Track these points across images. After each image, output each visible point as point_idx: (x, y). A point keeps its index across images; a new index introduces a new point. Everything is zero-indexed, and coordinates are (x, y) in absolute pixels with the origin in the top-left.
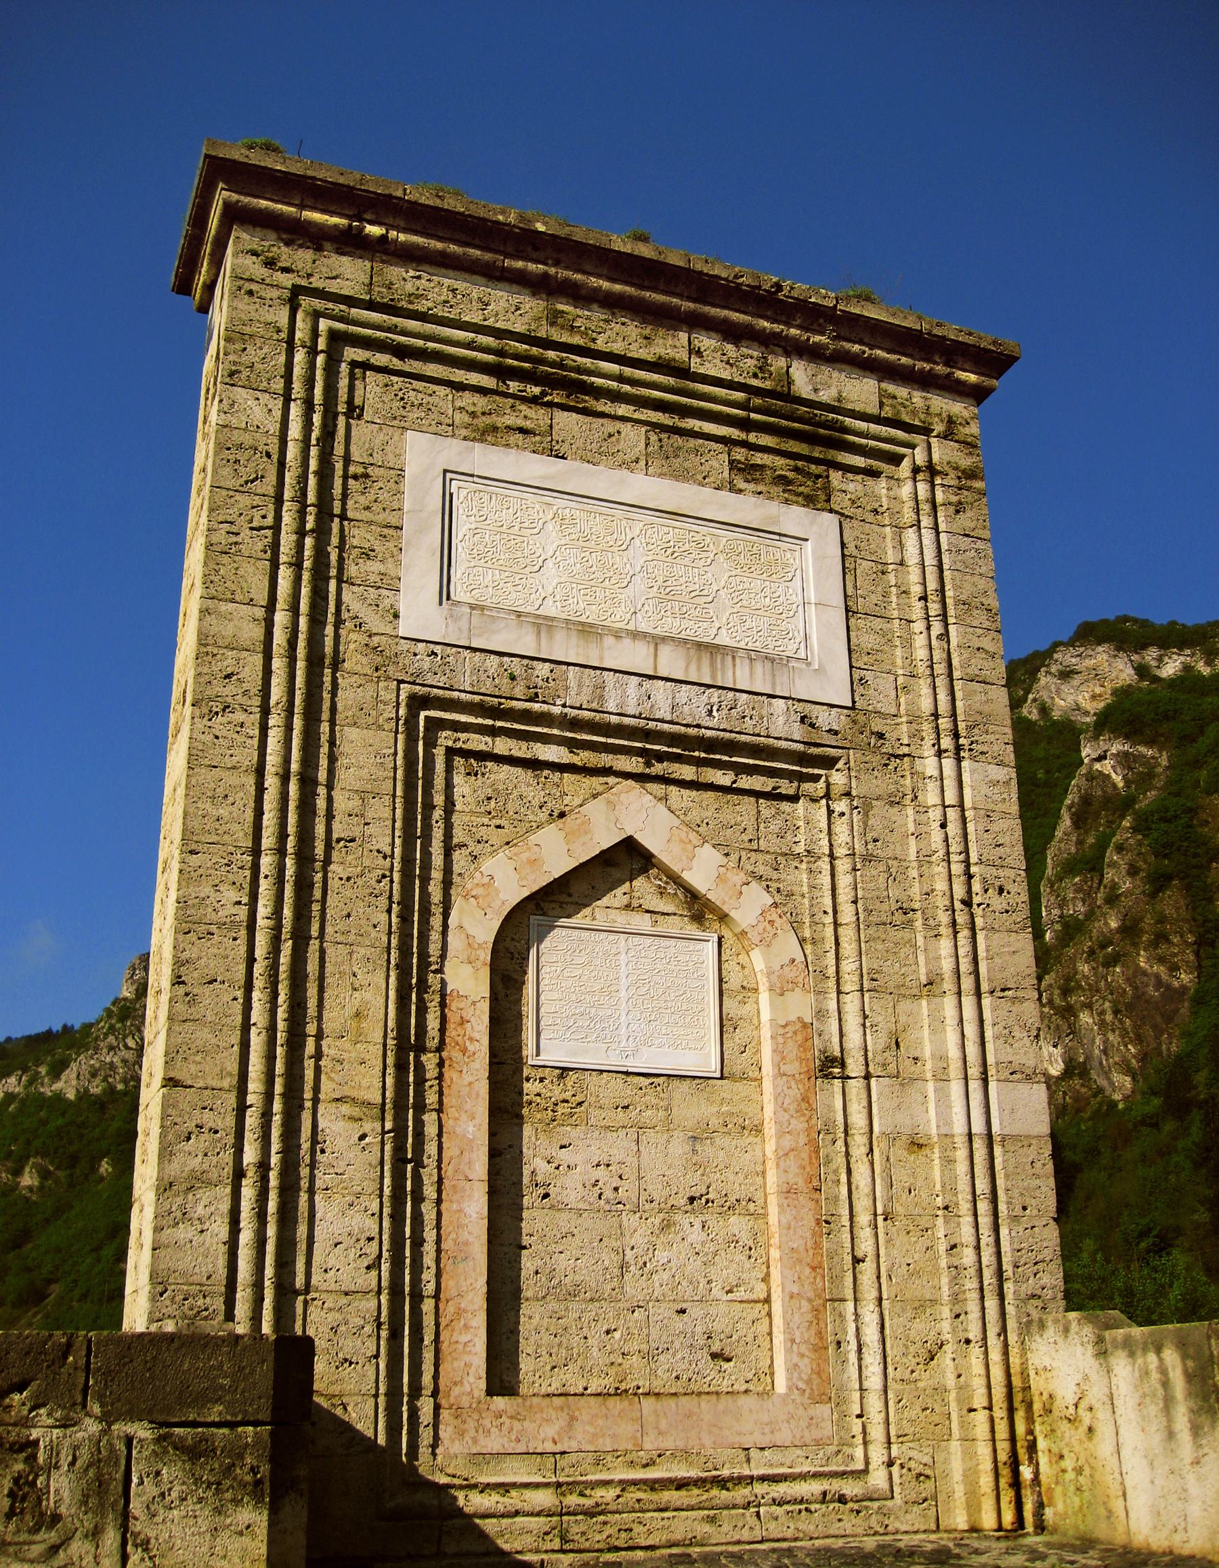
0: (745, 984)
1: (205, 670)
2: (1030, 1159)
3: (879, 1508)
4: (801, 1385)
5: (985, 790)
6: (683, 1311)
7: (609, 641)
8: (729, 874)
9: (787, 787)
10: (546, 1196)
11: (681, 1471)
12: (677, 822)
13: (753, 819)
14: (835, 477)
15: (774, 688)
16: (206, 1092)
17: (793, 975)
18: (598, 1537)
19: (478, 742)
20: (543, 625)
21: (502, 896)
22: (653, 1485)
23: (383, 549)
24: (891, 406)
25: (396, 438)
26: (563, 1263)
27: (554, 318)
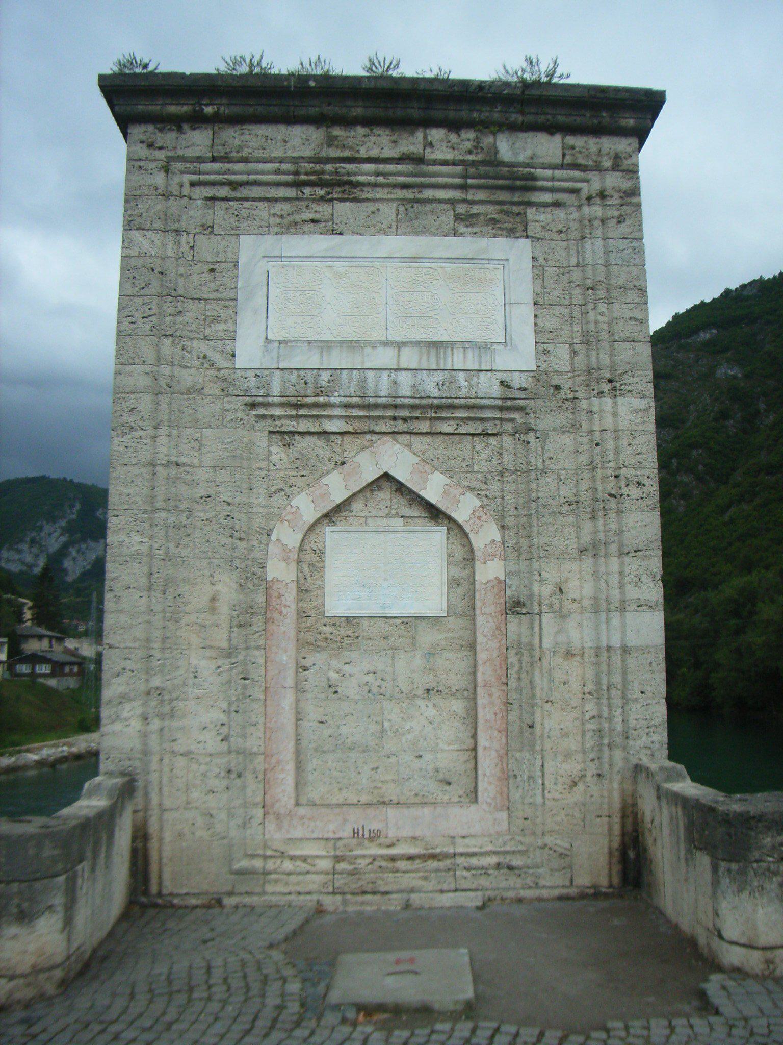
0: (465, 556)
1: (118, 408)
2: (649, 661)
3: (533, 873)
4: (489, 800)
5: (630, 416)
6: (421, 756)
7: (368, 350)
8: (451, 490)
9: (491, 428)
10: (336, 692)
11: (413, 850)
12: (417, 460)
13: (470, 453)
14: (531, 213)
15: (480, 366)
16: (127, 650)
17: (493, 550)
18: (354, 886)
19: (289, 425)
20: (326, 346)
21: (305, 519)
22: (393, 859)
23: (226, 315)
24: (573, 155)
25: (233, 242)
26: (344, 730)
27: (331, 141)
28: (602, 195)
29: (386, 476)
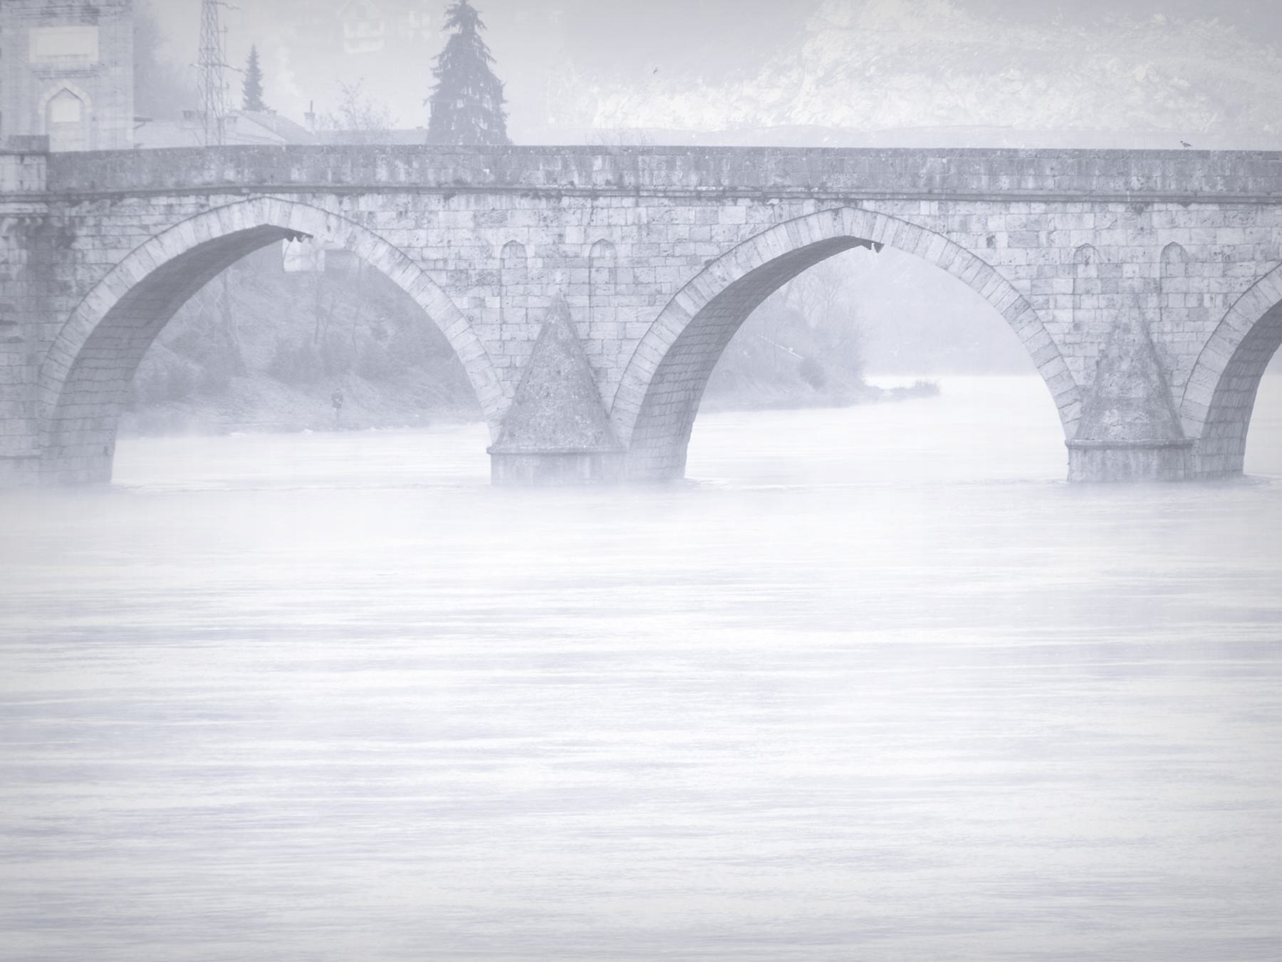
28: (115, 13)
29: (66, 89)
